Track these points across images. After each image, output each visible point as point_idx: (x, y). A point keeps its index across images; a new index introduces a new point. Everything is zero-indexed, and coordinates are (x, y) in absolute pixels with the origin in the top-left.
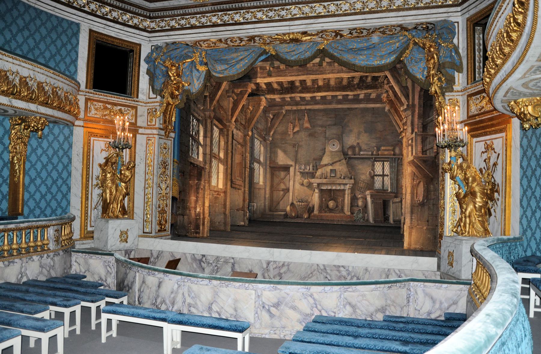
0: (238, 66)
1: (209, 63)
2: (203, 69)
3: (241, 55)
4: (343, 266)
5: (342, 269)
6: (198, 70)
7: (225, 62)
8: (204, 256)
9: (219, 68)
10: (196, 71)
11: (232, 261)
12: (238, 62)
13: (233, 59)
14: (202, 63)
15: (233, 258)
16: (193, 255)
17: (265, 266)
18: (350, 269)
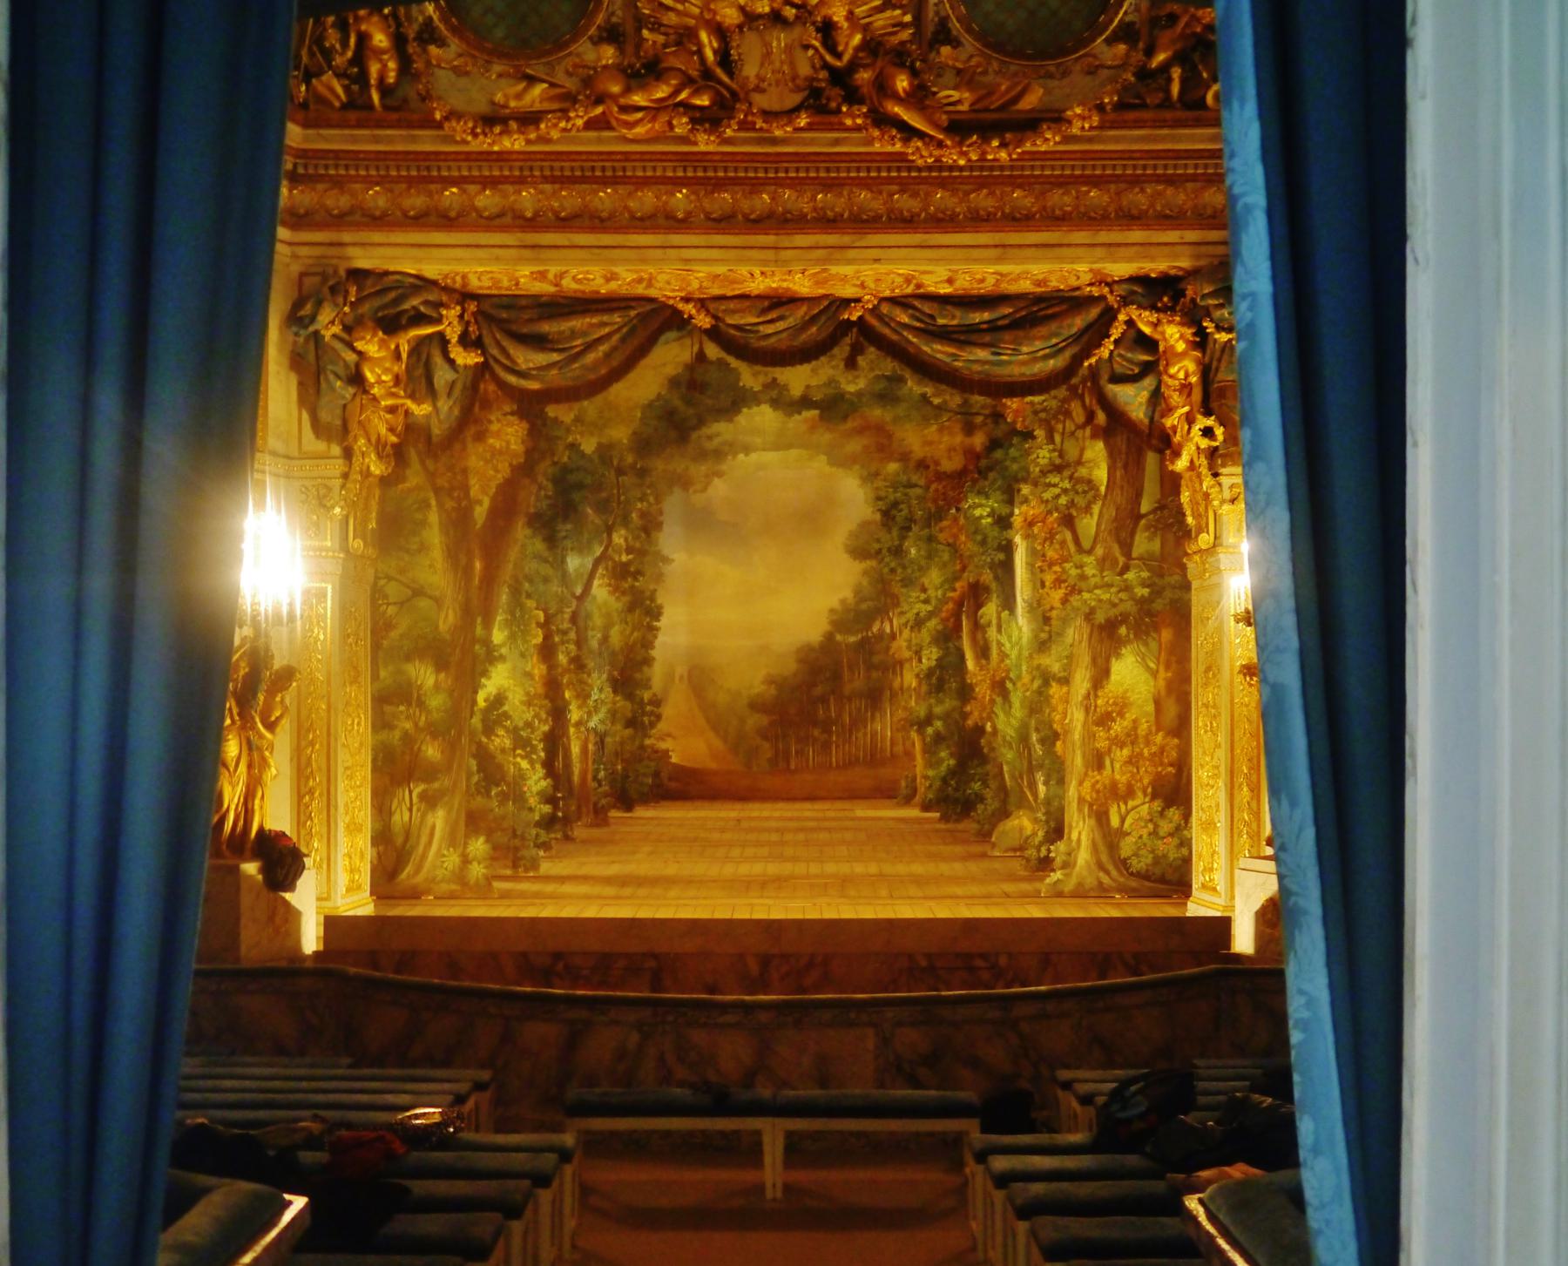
0: (590, 358)
1: (487, 340)
2: (467, 358)
3: (605, 324)
4: (983, 956)
5: (979, 963)
6: (452, 362)
7: (539, 342)
8: (557, 956)
9: (527, 358)
10: (446, 366)
11: (652, 964)
12: (589, 347)
13: (574, 334)
14: (464, 341)
15: (655, 956)
16: (524, 955)
17: (754, 967)
18: (1003, 961)
